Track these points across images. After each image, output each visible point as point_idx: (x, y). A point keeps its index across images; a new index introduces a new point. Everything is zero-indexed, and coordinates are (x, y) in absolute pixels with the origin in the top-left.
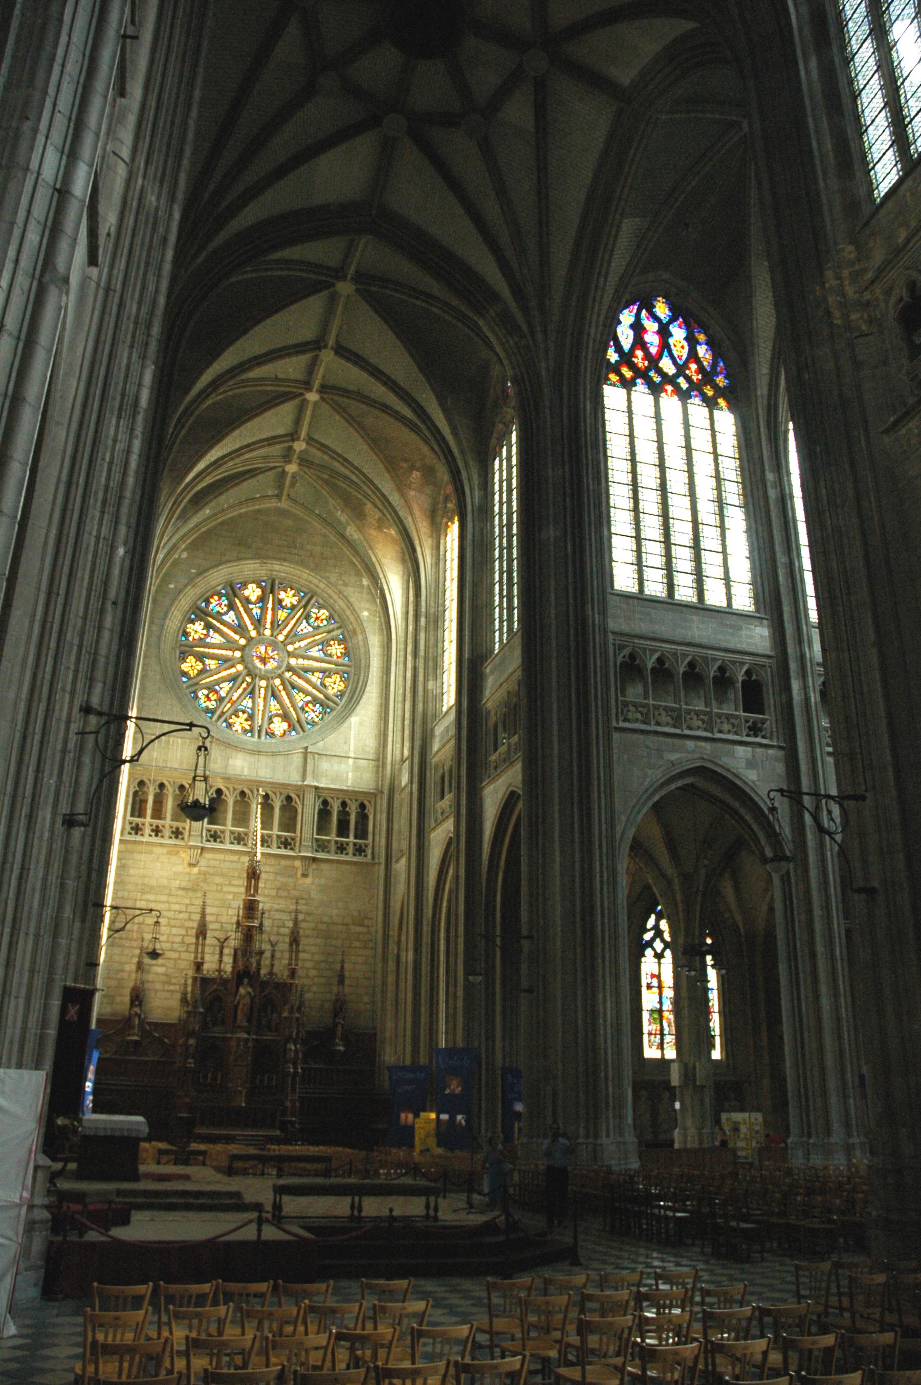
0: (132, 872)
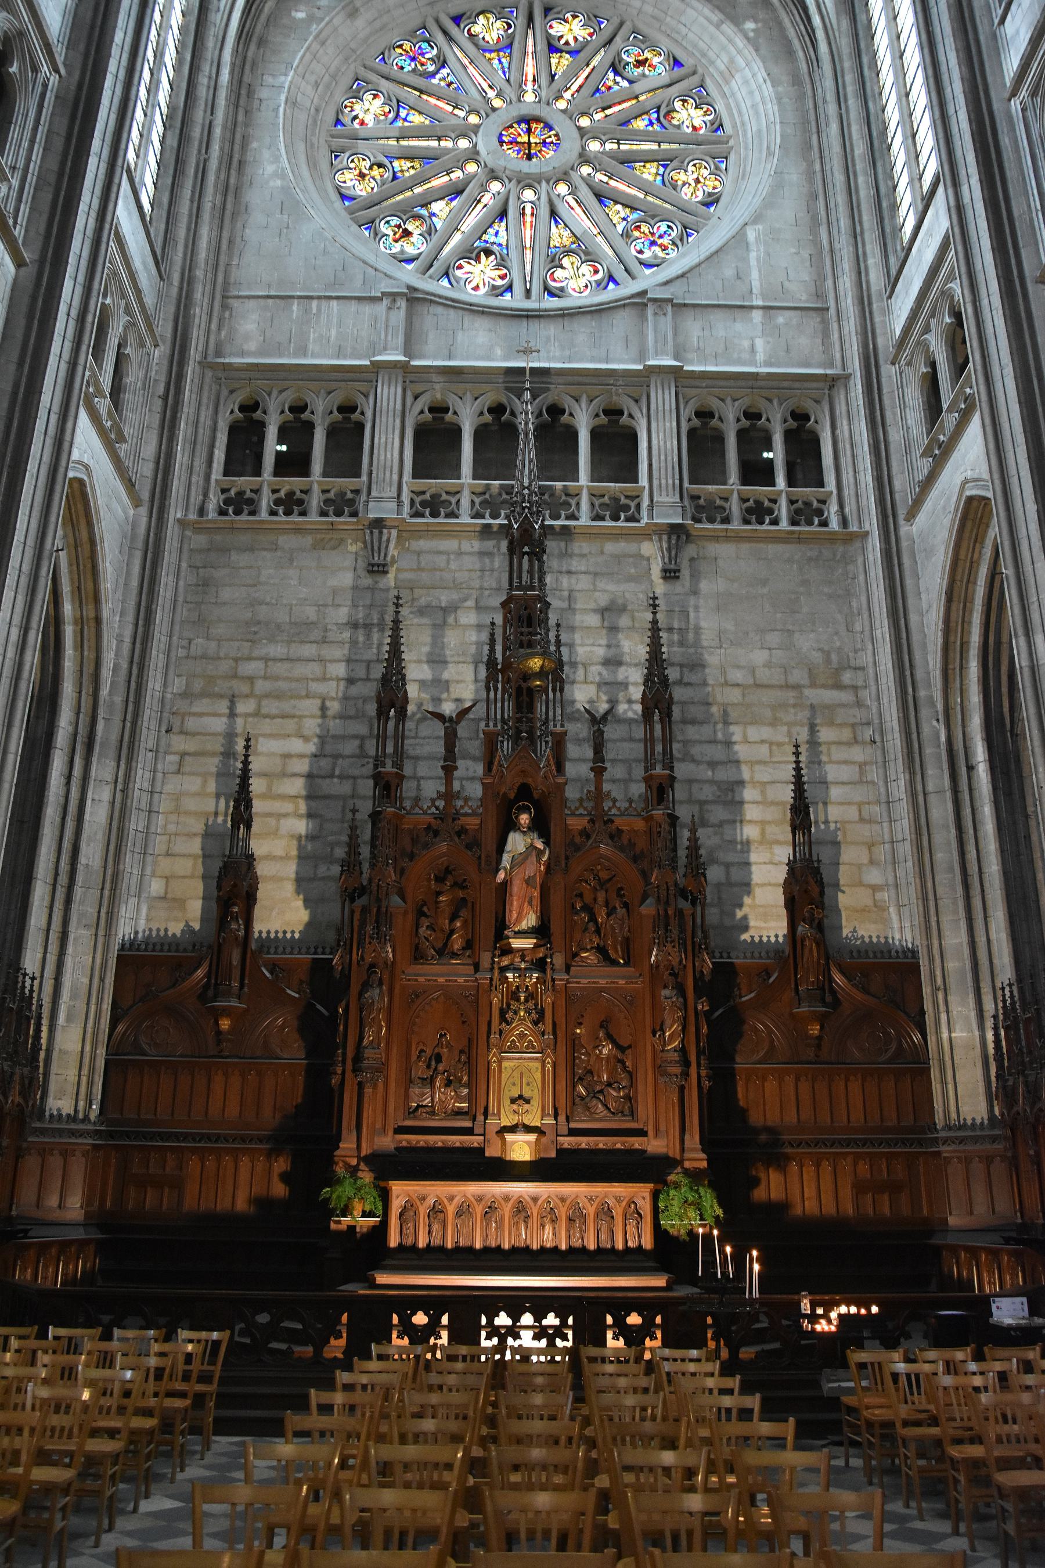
0: (226, 594)
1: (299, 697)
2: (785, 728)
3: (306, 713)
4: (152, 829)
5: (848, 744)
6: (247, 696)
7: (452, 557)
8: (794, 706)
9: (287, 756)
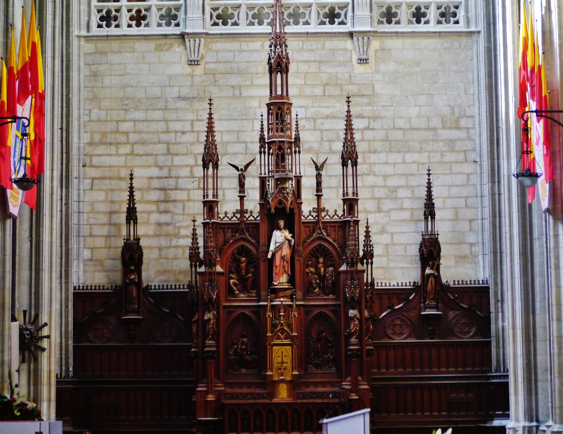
0: (107, 81)
1: (155, 143)
2: (427, 154)
3: (160, 153)
4: (81, 223)
5: (462, 162)
6: (125, 143)
7: (237, 53)
8: (432, 141)
9: (151, 178)
